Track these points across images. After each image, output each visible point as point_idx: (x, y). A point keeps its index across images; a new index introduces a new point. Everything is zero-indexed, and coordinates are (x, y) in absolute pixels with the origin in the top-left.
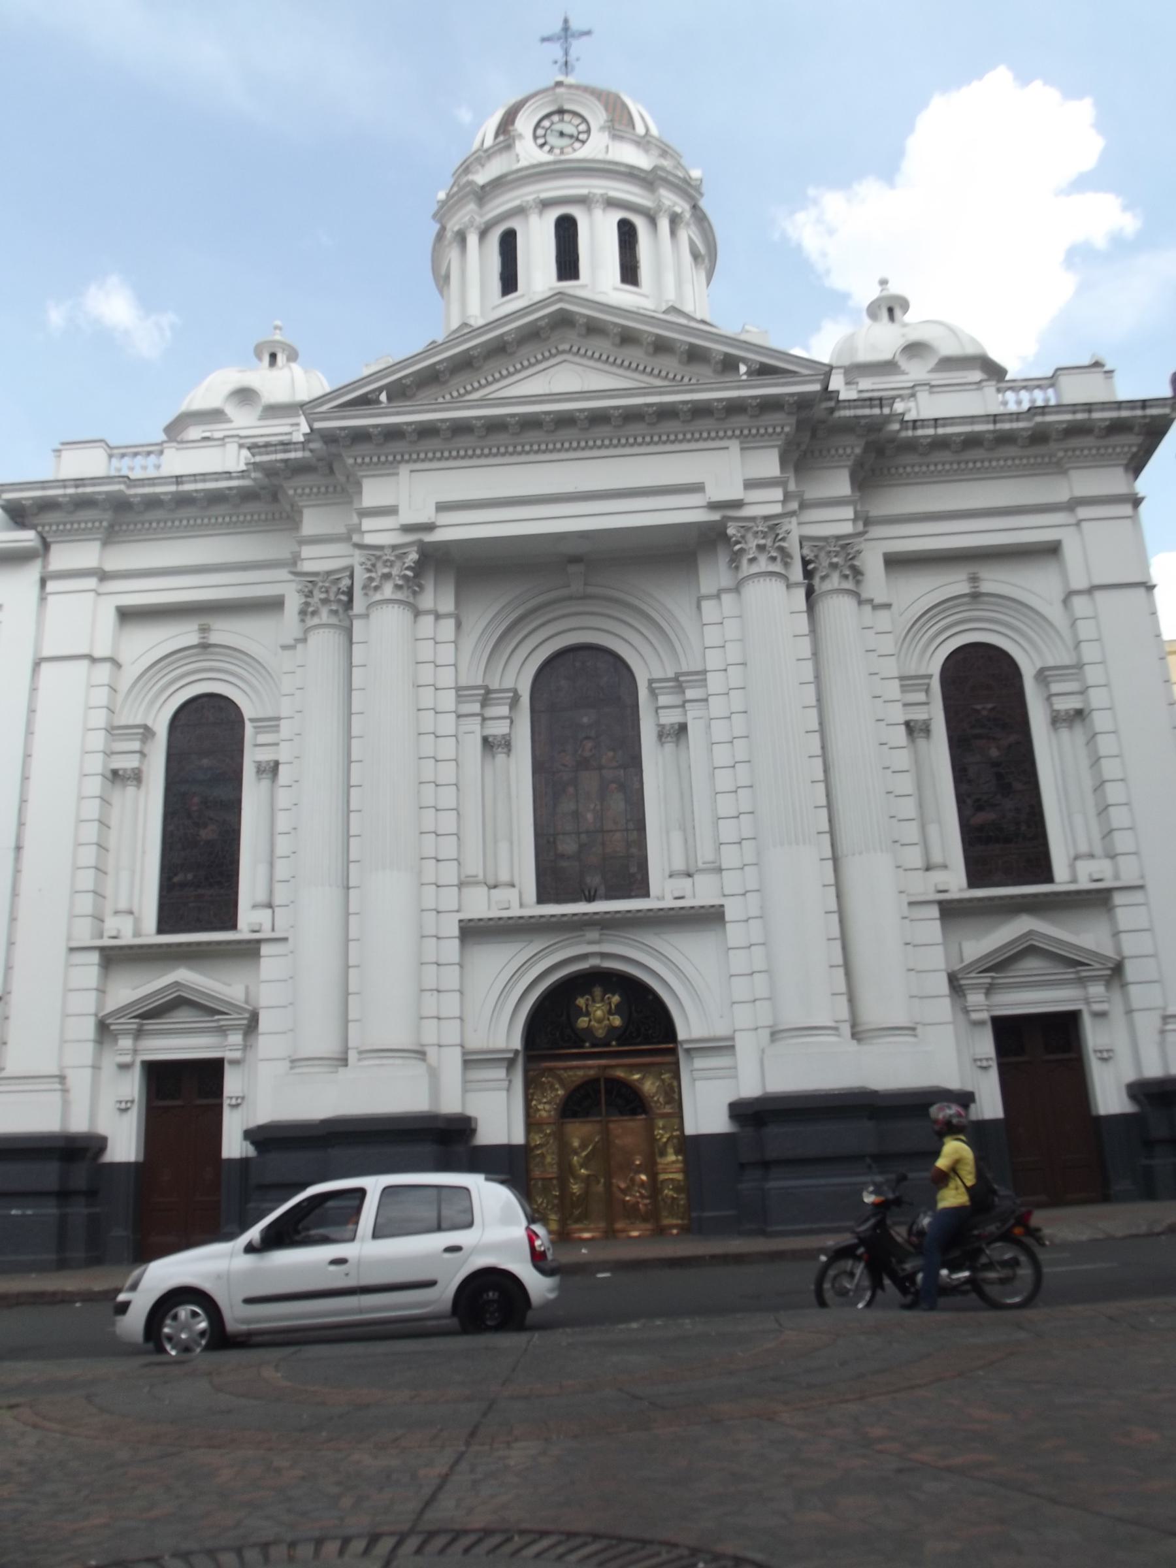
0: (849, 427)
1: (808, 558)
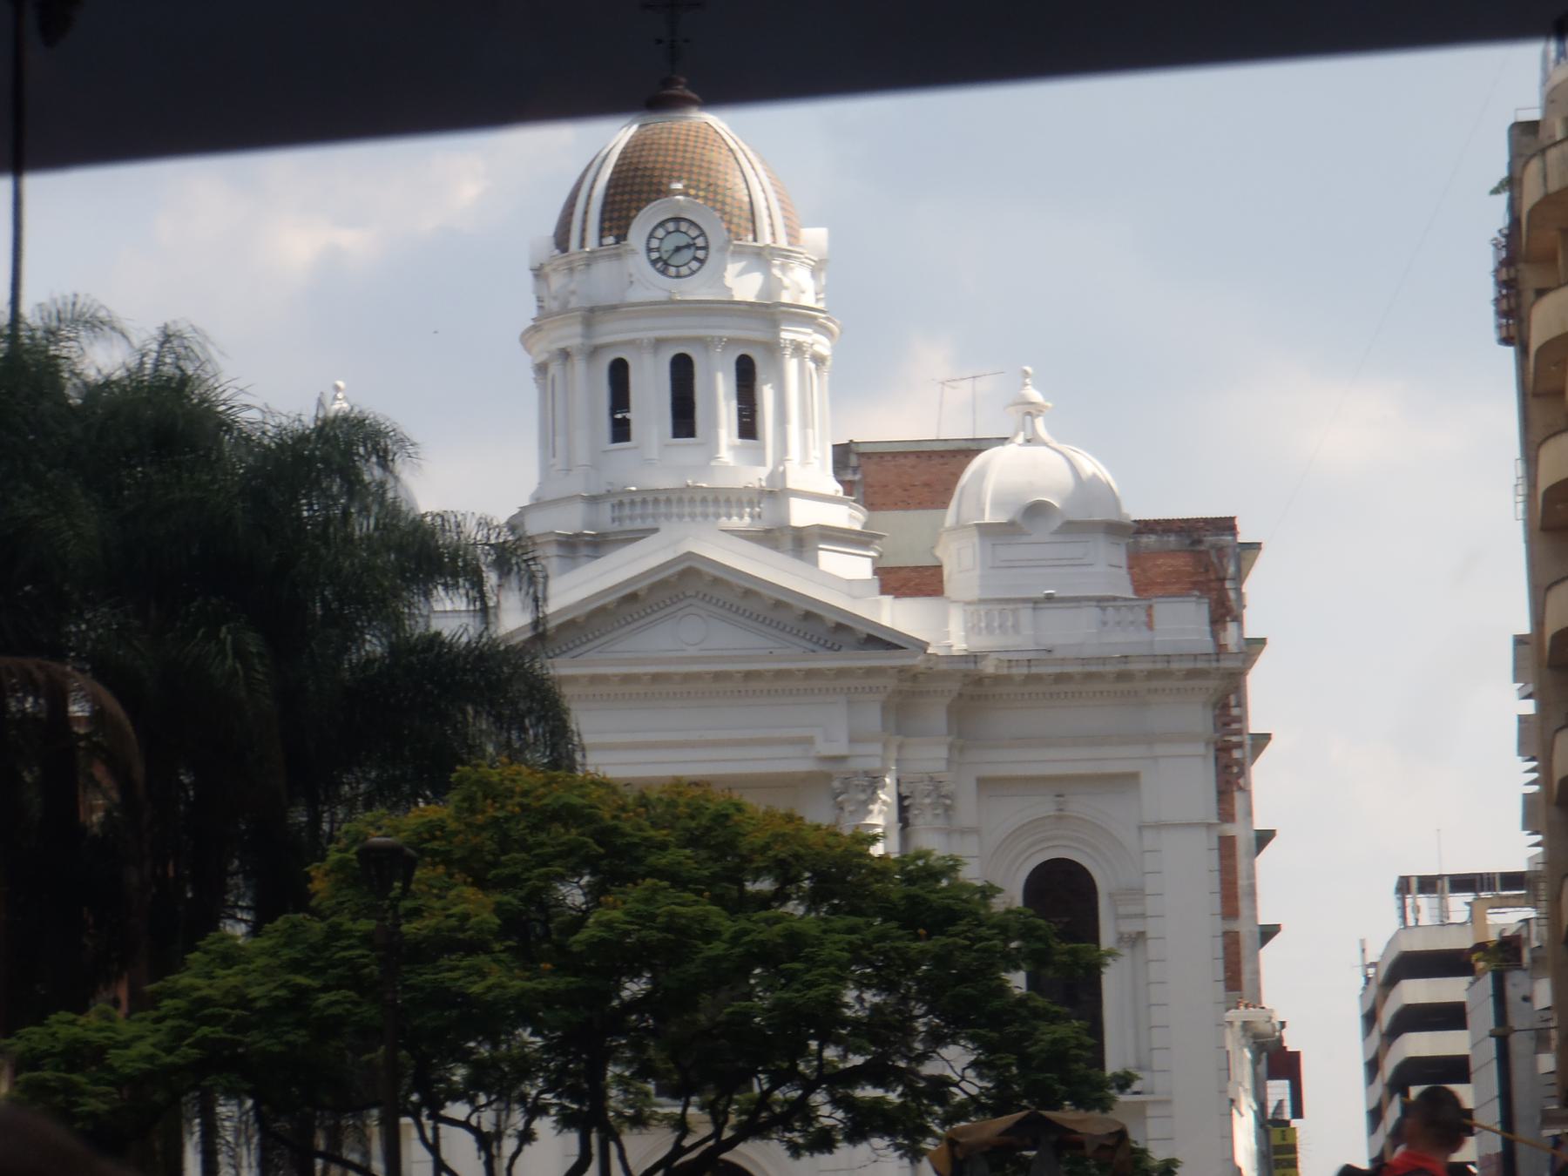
0: (945, 675)
1: (904, 795)
